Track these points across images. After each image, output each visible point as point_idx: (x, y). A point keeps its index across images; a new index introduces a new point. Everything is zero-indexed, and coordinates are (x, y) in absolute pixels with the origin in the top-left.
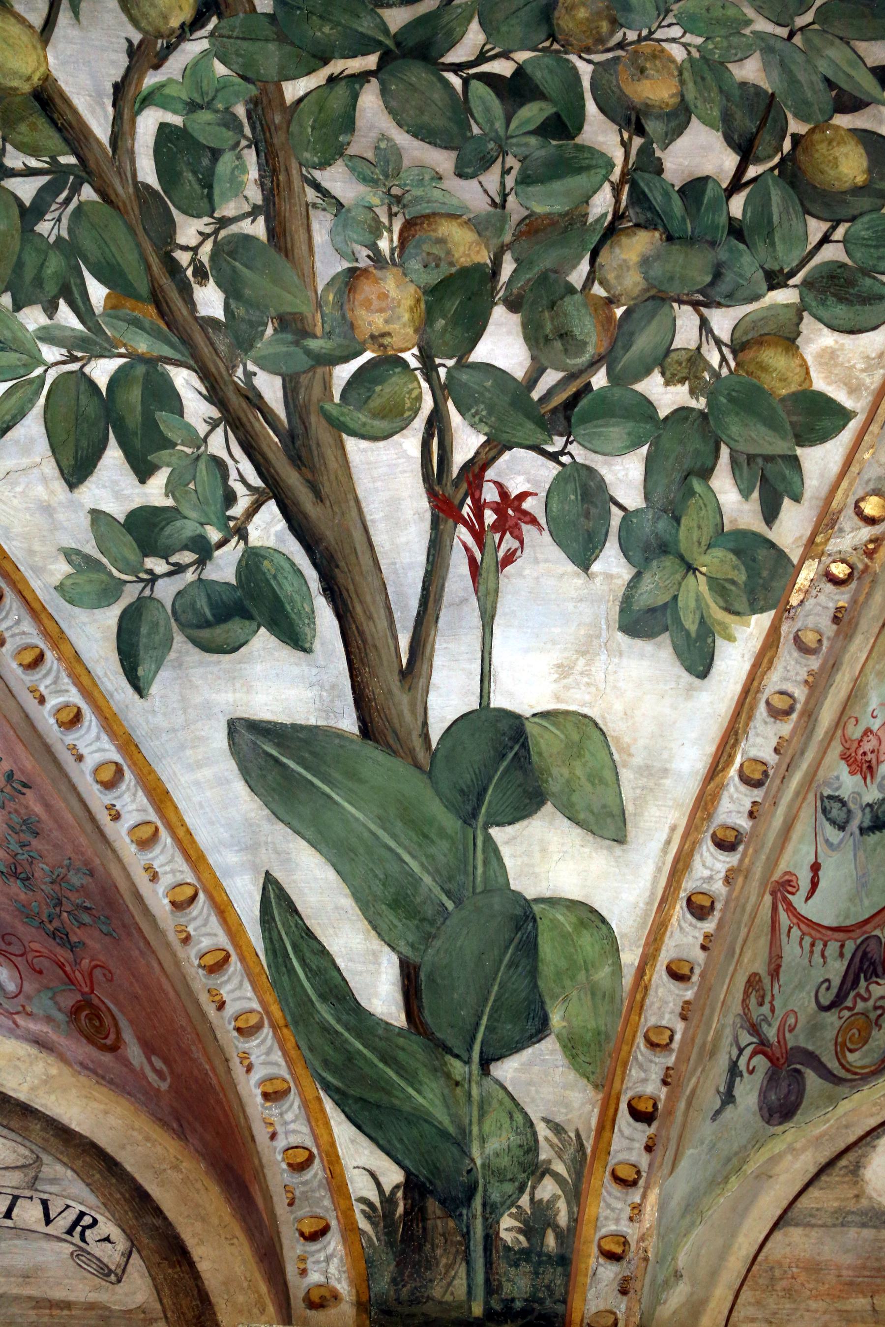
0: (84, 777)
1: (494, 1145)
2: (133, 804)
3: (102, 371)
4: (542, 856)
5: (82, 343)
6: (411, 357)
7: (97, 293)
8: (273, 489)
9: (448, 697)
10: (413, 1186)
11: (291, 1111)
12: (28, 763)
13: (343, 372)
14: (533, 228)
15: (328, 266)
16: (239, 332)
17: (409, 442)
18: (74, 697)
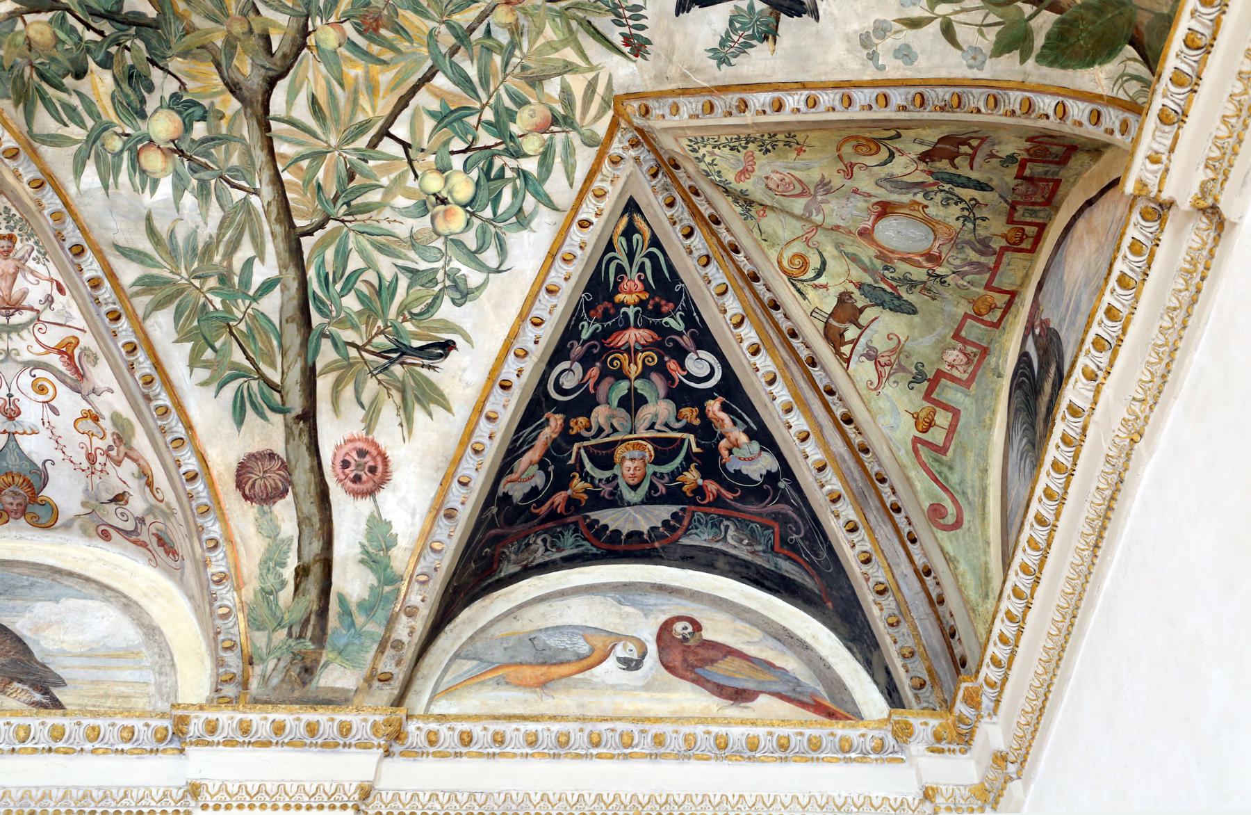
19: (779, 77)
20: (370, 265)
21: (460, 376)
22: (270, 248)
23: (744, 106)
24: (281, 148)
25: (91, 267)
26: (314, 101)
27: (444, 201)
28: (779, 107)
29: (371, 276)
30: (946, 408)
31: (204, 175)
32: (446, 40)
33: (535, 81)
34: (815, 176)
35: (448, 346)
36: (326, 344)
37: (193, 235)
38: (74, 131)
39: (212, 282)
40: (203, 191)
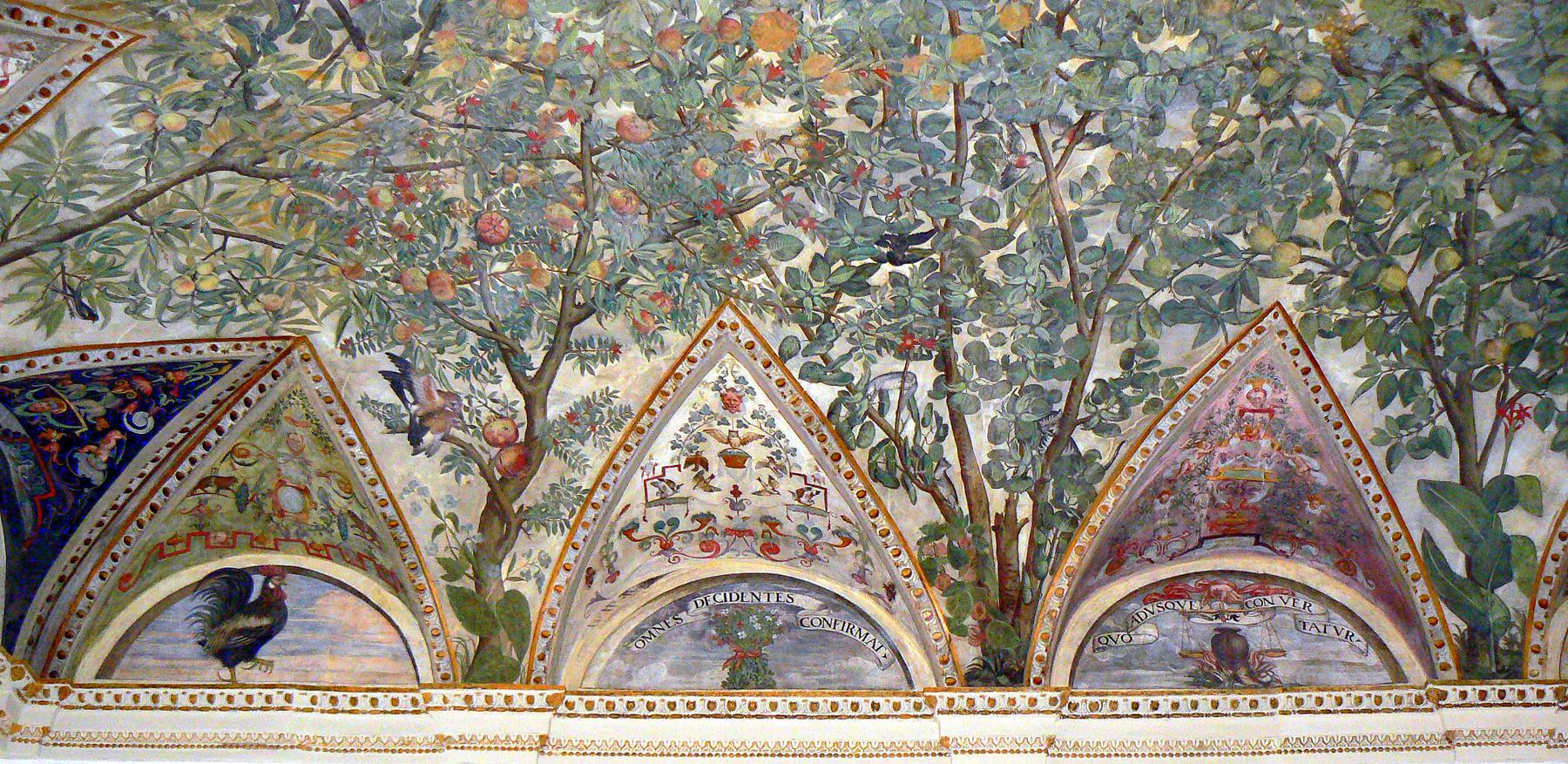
0: (1369, 500)
1: (1497, 616)
2: (1384, 507)
3: (1399, 374)
4: (1515, 522)
5: (1395, 365)
6: (1500, 366)
7: (1404, 349)
8: (1447, 408)
9: (1491, 471)
10: (1471, 630)
11: (1430, 604)
12: (1347, 492)
13: (1477, 371)
14: (1550, 326)
15: (1480, 338)
16: (1446, 360)
17: (1494, 393)
18: (1370, 474)
19: (369, 441)
20: (128, 257)
21: (77, 331)
22: (112, 201)
23: (341, 422)
24: (188, 185)
25: (36, 105)
26: (231, 193)
27: (194, 278)
28: (351, 443)
29: (120, 260)
30: (188, 544)
31: (147, 150)
32: (306, 248)
33: (297, 296)
34: (310, 458)
35: (93, 317)
36: (56, 253)
37: (99, 157)
38: (143, 76)
39: (65, 178)
40: (132, 154)
